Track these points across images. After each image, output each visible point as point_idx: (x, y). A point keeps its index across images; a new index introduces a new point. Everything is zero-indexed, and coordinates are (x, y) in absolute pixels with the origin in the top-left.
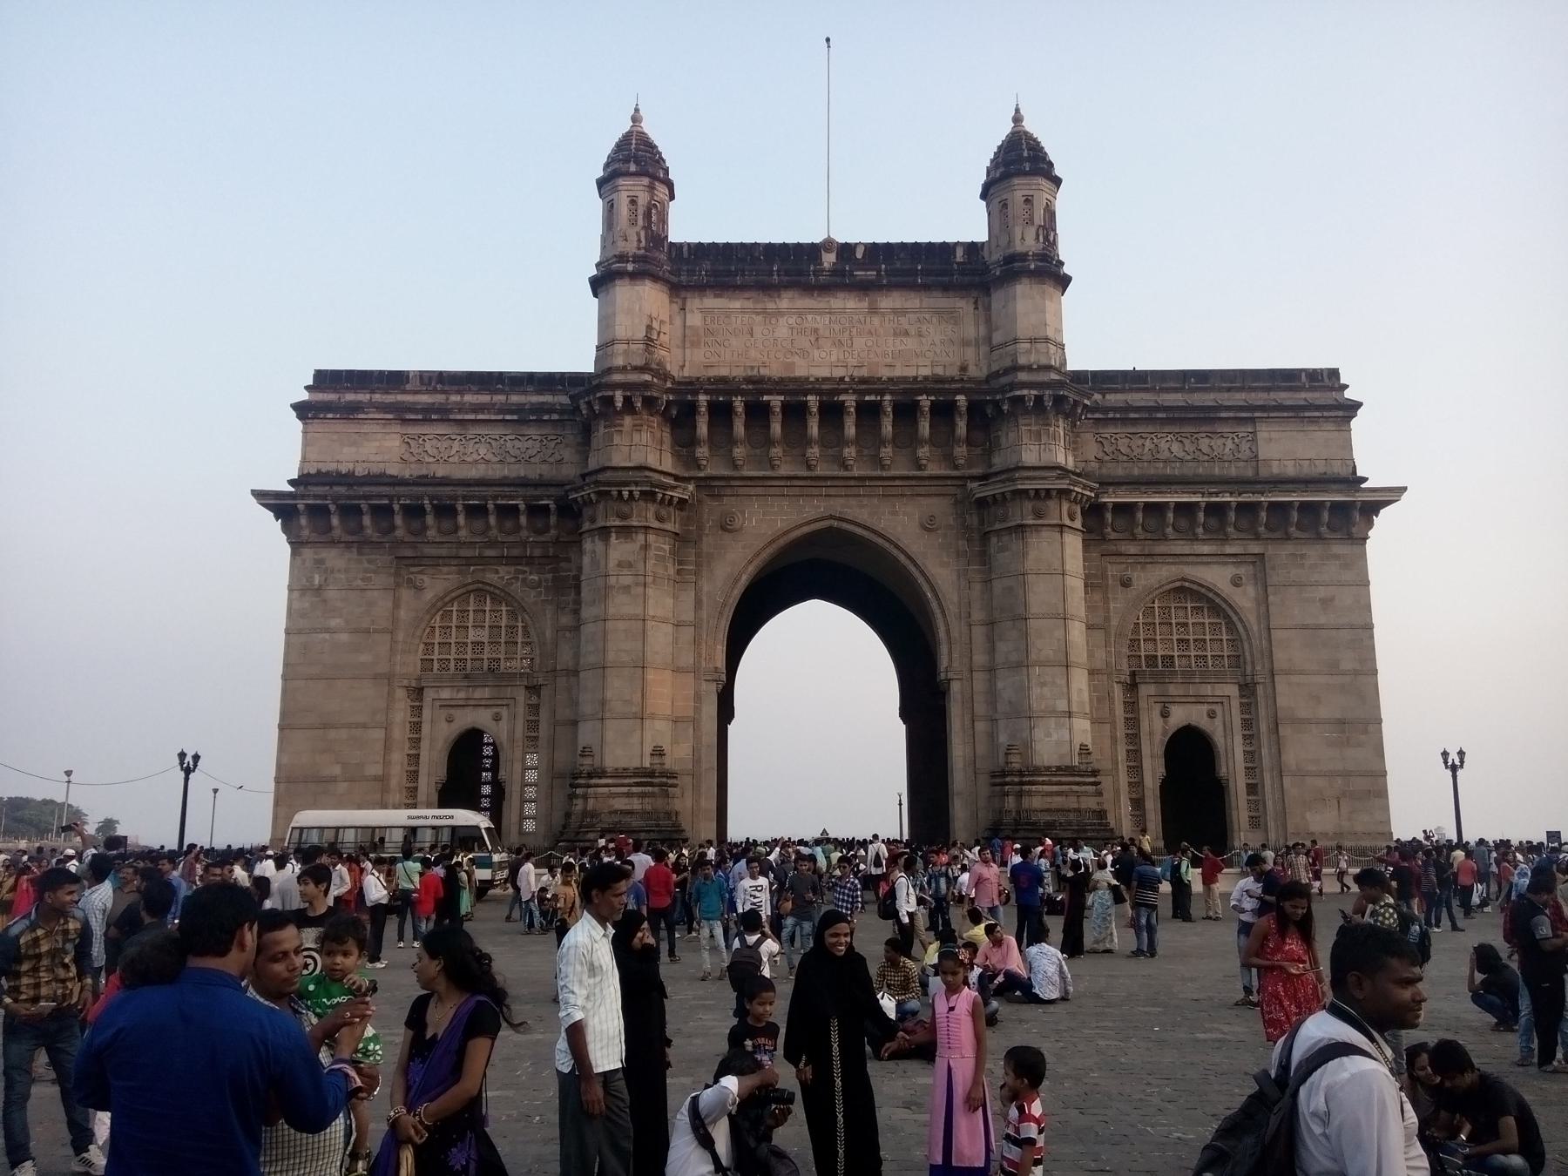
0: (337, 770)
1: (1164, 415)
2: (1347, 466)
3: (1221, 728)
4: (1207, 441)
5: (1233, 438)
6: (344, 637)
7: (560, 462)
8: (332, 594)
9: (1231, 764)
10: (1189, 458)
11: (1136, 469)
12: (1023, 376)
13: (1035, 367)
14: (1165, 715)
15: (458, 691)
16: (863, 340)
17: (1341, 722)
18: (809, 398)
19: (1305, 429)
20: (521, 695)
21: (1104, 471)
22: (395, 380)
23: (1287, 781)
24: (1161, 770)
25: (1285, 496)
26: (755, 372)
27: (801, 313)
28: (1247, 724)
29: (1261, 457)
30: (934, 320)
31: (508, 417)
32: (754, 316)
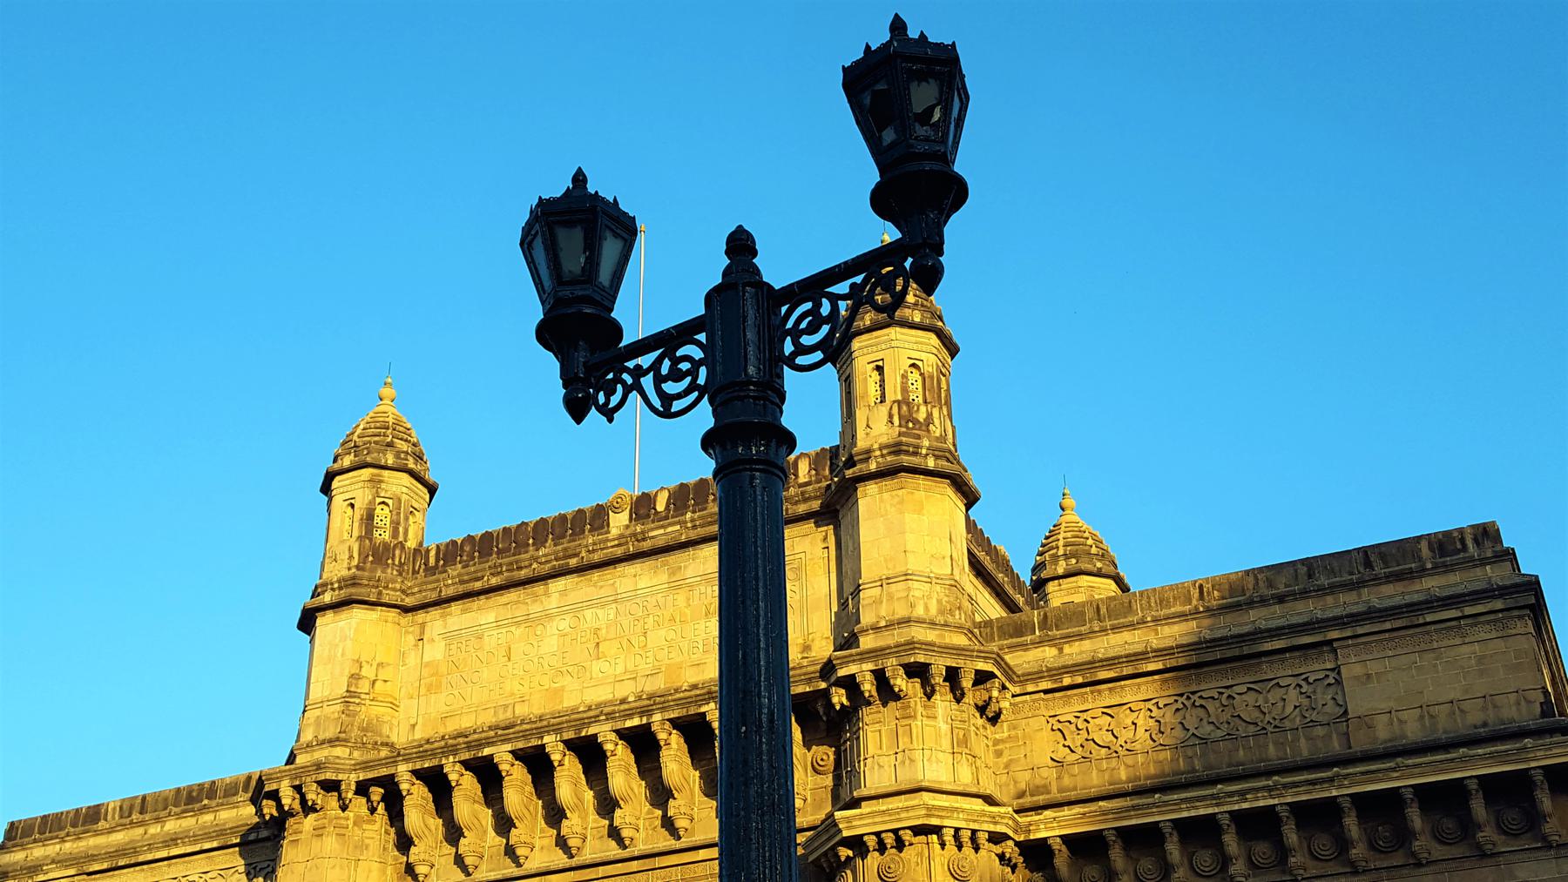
1: (1160, 666)
2: (1529, 702)
4: (1250, 697)
10: (1219, 733)
11: (1122, 768)
12: (867, 642)
13: (883, 624)
16: (662, 633)
18: (546, 739)
19: (1435, 645)
21: (1067, 781)
22: (91, 817)
25: (1381, 780)
26: (509, 714)
27: (576, 610)
31: (207, 846)
32: (513, 629)
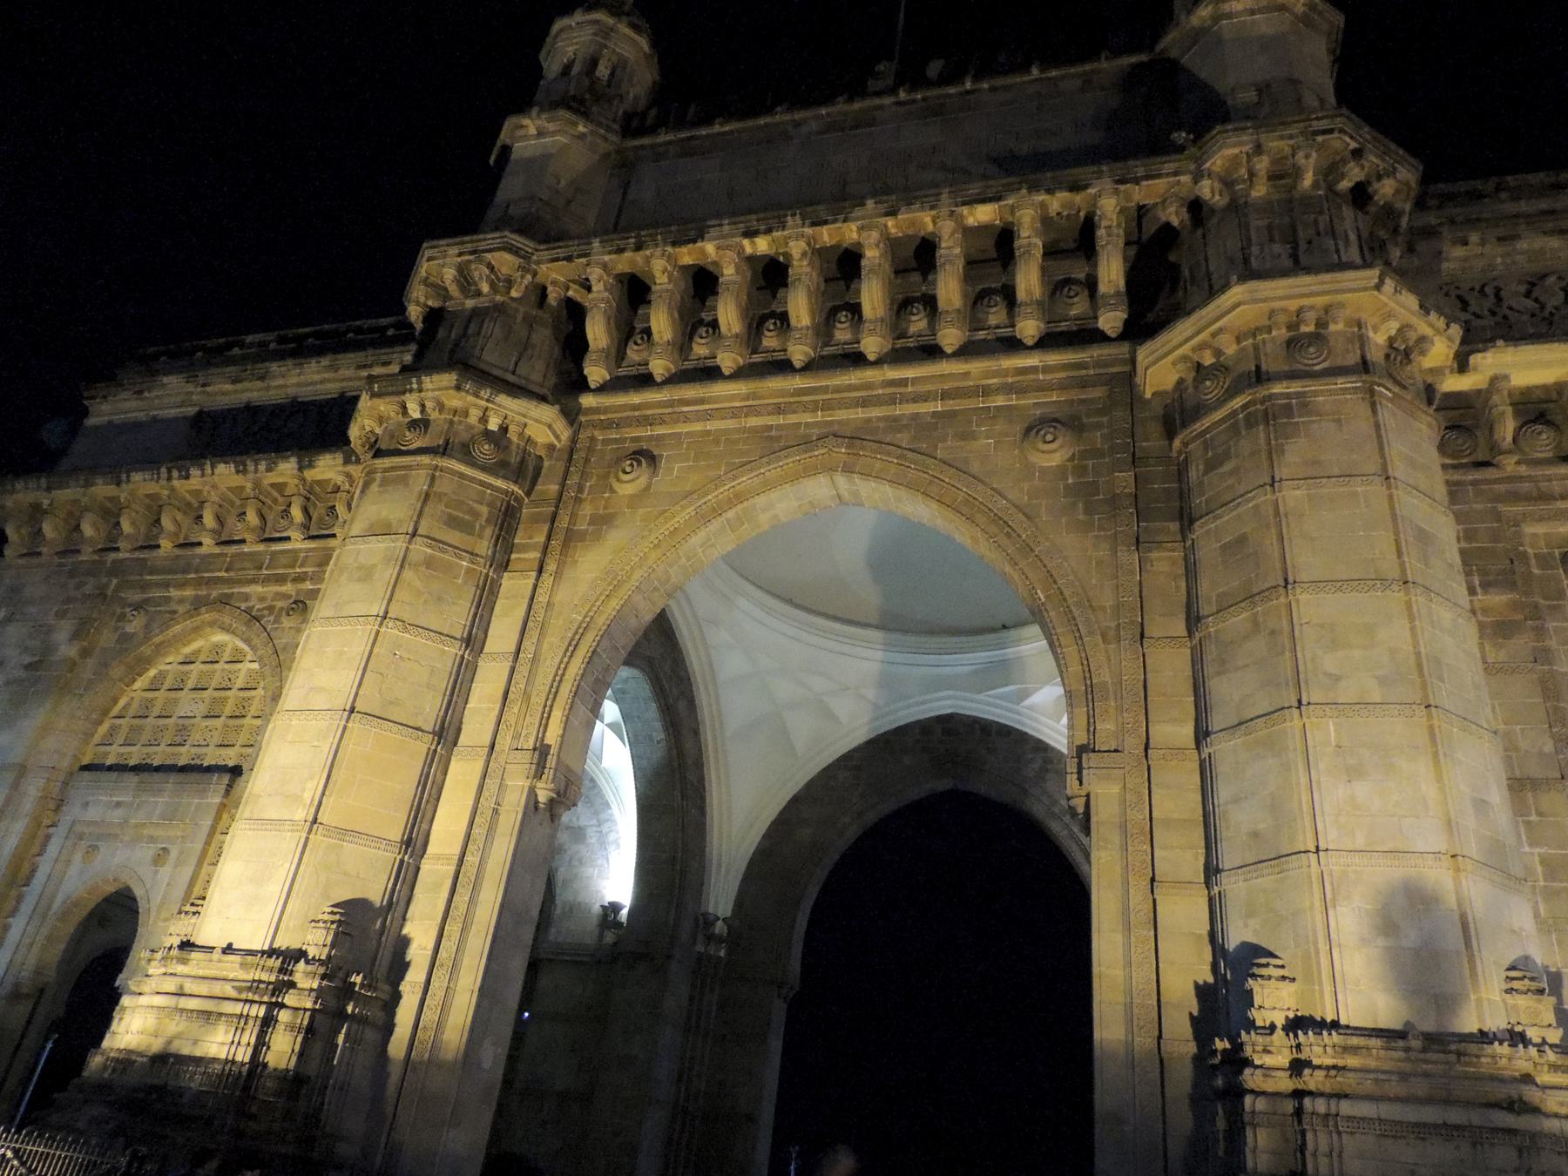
15: (118, 804)
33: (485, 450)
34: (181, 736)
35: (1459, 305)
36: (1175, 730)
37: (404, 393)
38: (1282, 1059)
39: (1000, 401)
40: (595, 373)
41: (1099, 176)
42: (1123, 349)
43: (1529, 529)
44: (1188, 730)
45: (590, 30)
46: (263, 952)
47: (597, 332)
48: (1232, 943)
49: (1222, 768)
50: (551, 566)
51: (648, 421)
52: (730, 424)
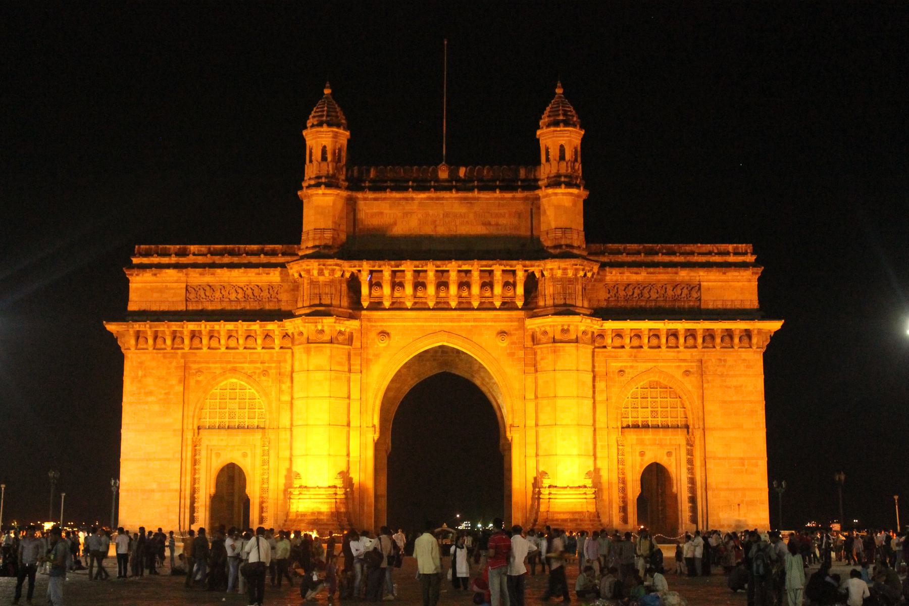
0: (154, 486)
3: (674, 462)
5: (687, 288)
6: (156, 408)
7: (279, 301)
8: (149, 380)
9: (679, 485)
14: (642, 454)
15: (222, 440)
17: (742, 459)
20: (259, 443)
23: (709, 493)
24: (638, 490)
28: (690, 462)
29: (704, 297)
30: (507, 215)
33: (341, 338)
34: (232, 416)
35: (608, 291)
36: (531, 422)
37: (316, 323)
38: (547, 492)
39: (489, 324)
40: (365, 304)
41: (518, 264)
42: (522, 314)
43: (613, 364)
44: (533, 423)
45: (331, 135)
46: (325, 488)
47: (365, 290)
48: (540, 471)
49: (540, 434)
50: (364, 371)
51: (383, 320)
52: (411, 324)
